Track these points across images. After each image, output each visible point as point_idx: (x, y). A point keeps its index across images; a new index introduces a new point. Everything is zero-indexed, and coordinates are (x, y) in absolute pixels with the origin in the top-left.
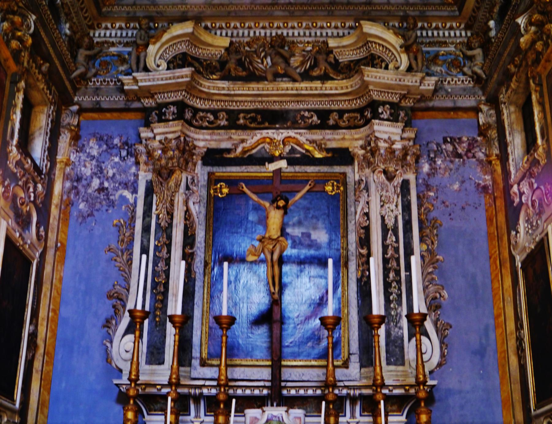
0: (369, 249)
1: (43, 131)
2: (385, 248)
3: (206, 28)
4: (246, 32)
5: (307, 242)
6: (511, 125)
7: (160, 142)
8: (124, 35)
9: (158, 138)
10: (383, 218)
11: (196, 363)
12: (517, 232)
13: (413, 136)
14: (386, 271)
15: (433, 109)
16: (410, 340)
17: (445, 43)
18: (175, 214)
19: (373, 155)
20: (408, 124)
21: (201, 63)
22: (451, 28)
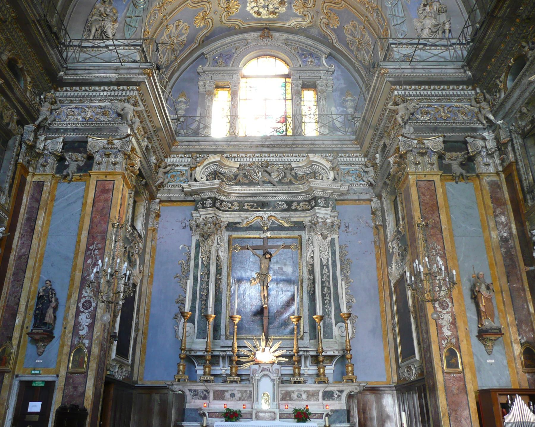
0: (314, 276)
1: (142, 215)
2: (322, 275)
3: (227, 157)
4: (248, 159)
5: (282, 272)
6: (388, 210)
7: (203, 219)
8: (183, 161)
9: (202, 217)
10: (321, 259)
11: (223, 337)
12: (392, 268)
13: (337, 215)
14: (323, 288)
15: (347, 200)
16: (336, 325)
17: (353, 164)
18: (211, 258)
19: (315, 225)
20: (334, 208)
21: (224, 176)
22: (356, 156)
